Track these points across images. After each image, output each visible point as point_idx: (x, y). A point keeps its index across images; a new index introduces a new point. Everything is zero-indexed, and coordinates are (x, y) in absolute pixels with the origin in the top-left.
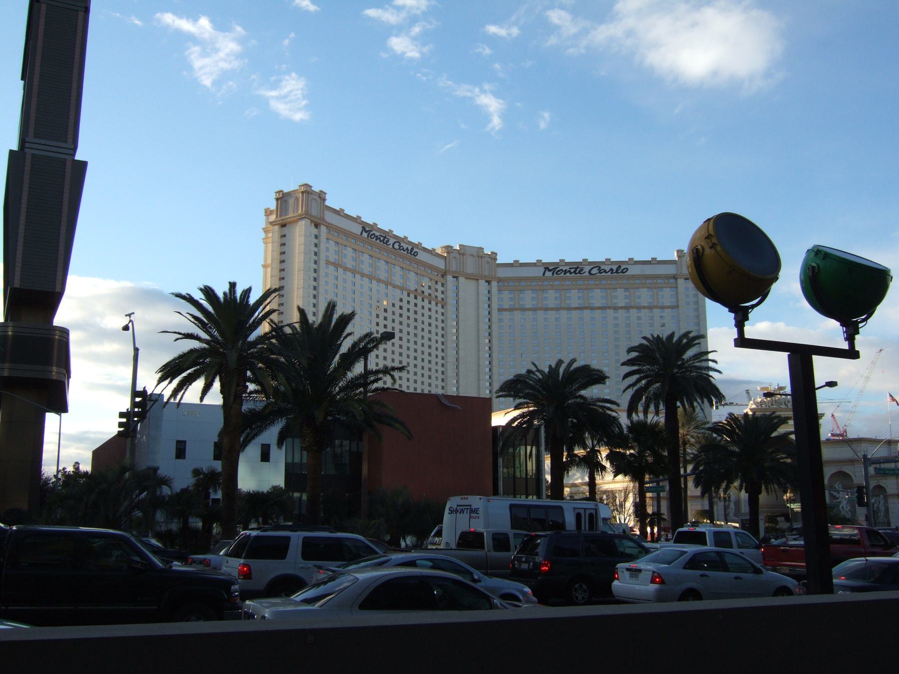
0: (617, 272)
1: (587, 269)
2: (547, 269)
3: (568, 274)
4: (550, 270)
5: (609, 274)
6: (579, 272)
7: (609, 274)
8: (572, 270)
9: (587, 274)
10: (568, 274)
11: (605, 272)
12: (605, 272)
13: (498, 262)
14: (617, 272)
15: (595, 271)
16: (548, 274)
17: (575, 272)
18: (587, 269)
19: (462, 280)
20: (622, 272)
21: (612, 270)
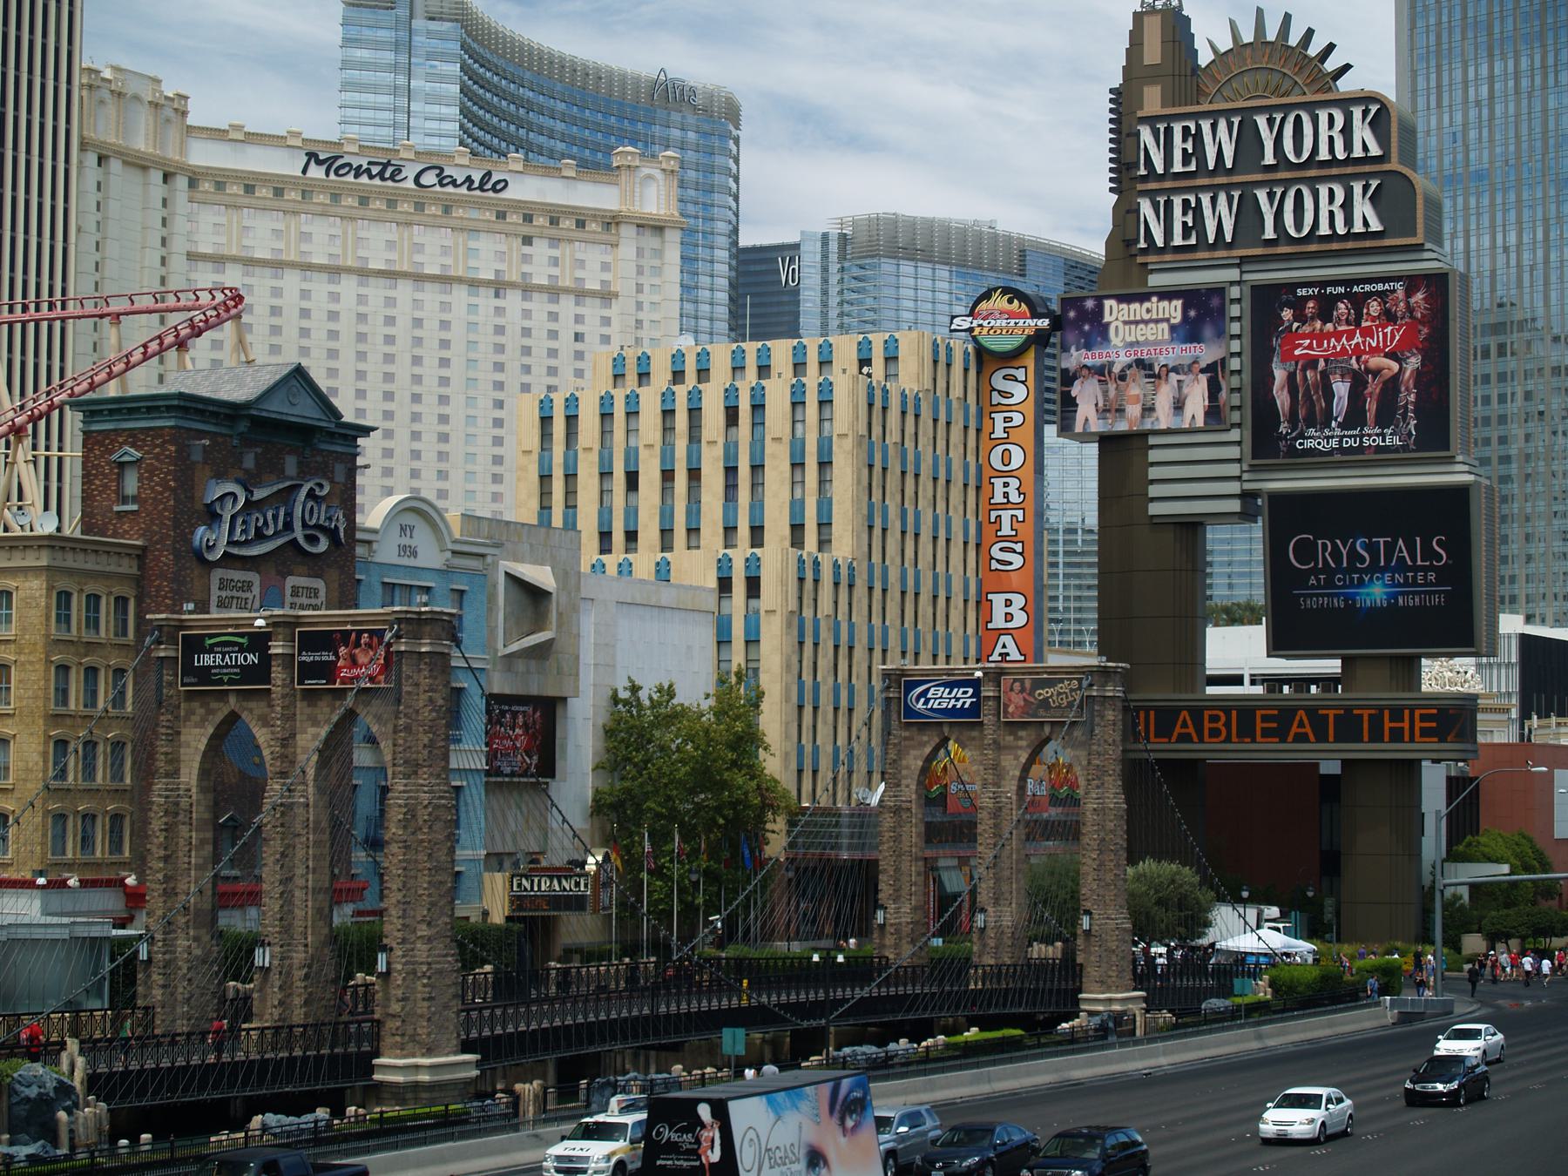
0: (481, 188)
1: (410, 172)
2: (312, 156)
3: (364, 179)
4: (319, 162)
5: (463, 190)
6: (392, 178)
7: (463, 190)
8: (375, 170)
9: (410, 184)
10: (364, 179)
11: (454, 183)
12: (454, 183)
13: (190, 121)
14: (481, 188)
15: (429, 179)
16: (316, 172)
17: (381, 175)
18: (410, 172)
19: (115, 165)
20: (494, 189)
21: (469, 179)
